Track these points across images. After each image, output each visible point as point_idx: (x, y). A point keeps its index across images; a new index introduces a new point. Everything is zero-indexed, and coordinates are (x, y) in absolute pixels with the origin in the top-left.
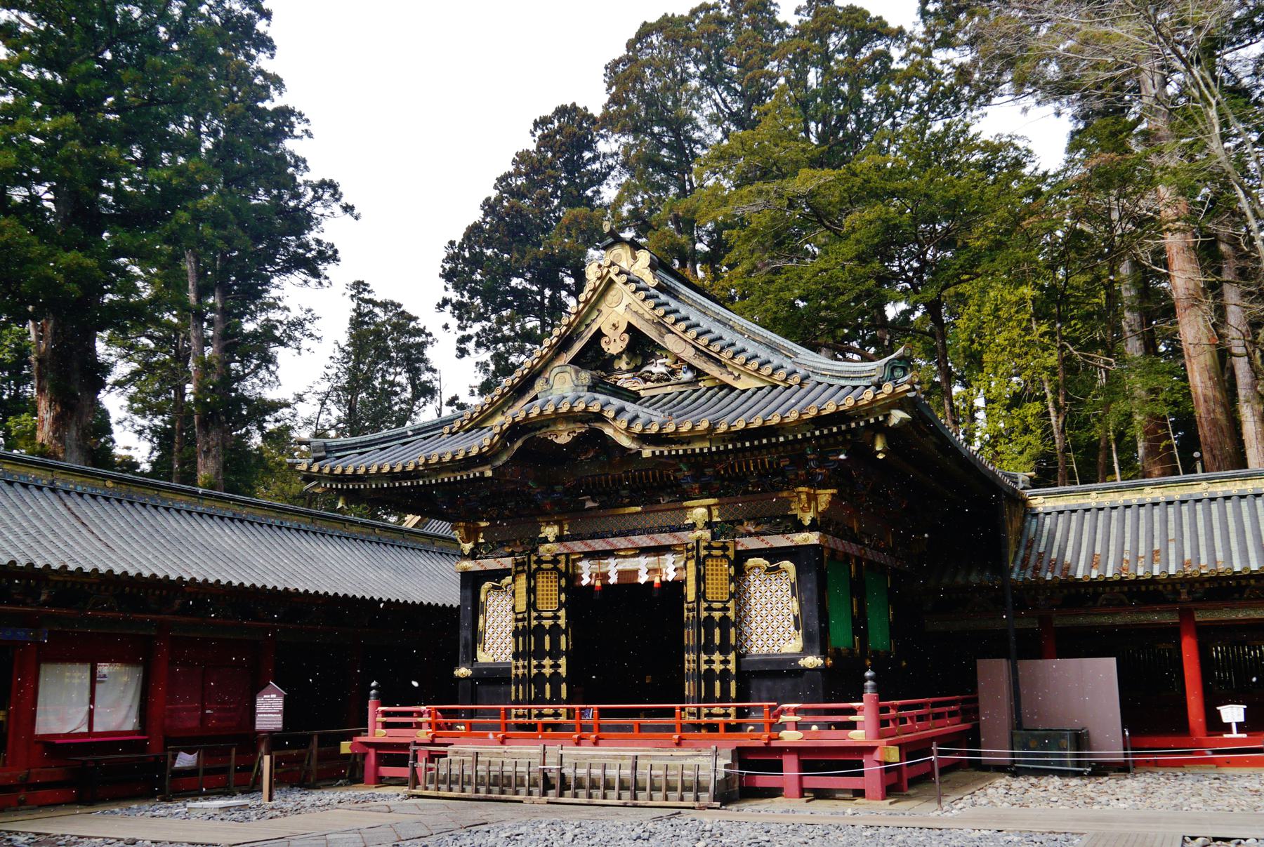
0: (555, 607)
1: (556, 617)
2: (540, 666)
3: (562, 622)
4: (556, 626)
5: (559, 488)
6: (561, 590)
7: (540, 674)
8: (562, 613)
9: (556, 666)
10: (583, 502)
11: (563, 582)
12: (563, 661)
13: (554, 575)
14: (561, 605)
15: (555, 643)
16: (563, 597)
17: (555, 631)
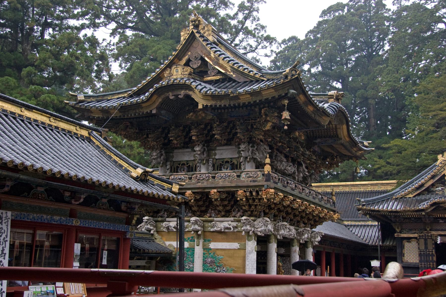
0: (432, 248)
1: (432, 252)
2: (430, 265)
3: (434, 253)
4: (432, 254)
5: (431, 217)
6: (433, 244)
7: (430, 267)
8: (434, 250)
9: (433, 265)
10: (439, 221)
11: (433, 242)
12: (435, 264)
13: (431, 240)
14: (433, 248)
15: (432, 258)
16: (434, 246)
17: (432, 255)
